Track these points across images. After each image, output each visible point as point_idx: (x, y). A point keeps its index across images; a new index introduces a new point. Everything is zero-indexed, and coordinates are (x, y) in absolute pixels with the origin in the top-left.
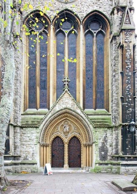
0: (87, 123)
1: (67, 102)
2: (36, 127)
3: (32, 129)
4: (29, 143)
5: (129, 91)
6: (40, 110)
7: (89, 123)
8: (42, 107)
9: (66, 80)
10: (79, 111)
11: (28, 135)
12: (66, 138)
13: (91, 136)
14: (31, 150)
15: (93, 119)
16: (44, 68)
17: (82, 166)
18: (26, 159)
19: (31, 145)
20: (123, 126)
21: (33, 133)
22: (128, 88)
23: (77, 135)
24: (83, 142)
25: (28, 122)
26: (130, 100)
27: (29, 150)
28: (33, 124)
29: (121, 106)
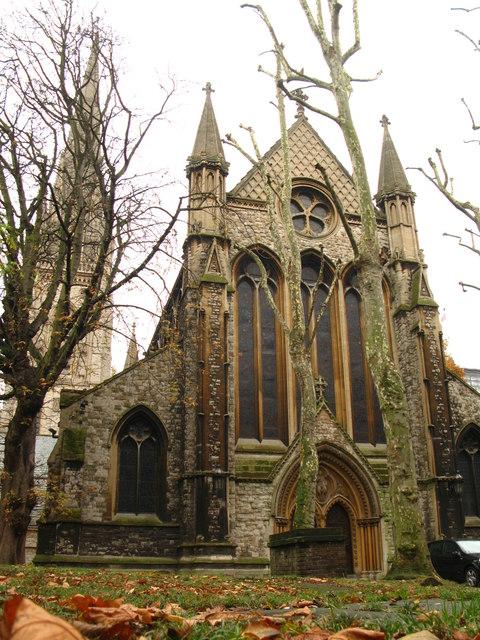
0: (366, 473)
1: (327, 431)
2: (269, 482)
3: (258, 485)
4: (252, 517)
5: (441, 415)
6: (266, 442)
7: (370, 474)
8: (270, 435)
9: (321, 383)
10: (349, 448)
11: (251, 499)
12: (322, 506)
13: (376, 503)
14: (257, 532)
15: (378, 466)
16: (269, 353)
17: (357, 569)
18: (245, 553)
19: (256, 523)
20: (439, 481)
21: (261, 494)
22: (440, 409)
23: (344, 499)
24: (358, 514)
25: (246, 468)
26: (446, 431)
27: (251, 533)
28: (259, 475)
29: (430, 443)
